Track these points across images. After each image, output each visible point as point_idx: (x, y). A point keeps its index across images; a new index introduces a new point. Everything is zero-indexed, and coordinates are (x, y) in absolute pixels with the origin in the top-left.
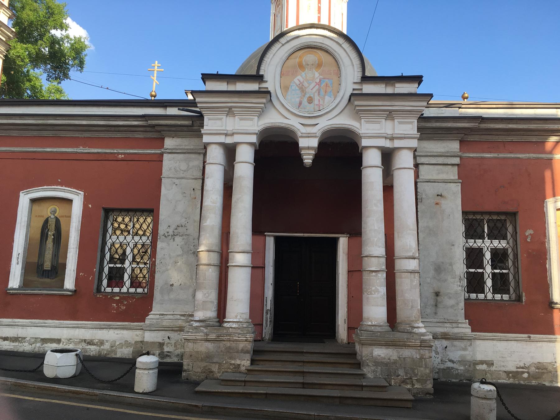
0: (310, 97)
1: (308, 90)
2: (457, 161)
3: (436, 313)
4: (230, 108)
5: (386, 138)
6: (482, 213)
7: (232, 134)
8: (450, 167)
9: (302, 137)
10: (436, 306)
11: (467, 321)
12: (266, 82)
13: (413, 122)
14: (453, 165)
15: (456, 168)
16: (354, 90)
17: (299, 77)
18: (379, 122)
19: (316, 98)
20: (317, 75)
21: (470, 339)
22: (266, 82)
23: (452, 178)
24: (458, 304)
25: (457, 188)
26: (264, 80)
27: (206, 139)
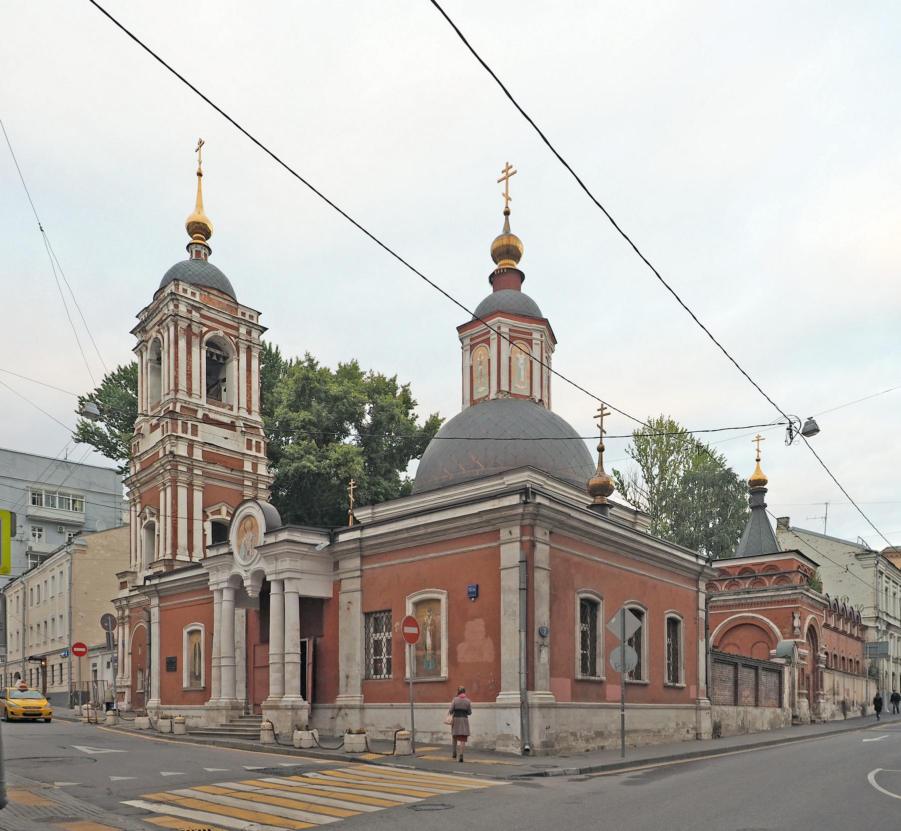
0: (248, 551)
1: (247, 546)
2: (358, 573)
3: (347, 691)
4: (216, 566)
5: (276, 573)
6: (380, 612)
7: (218, 584)
8: (356, 578)
9: (245, 579)
10: (347, 685)
11: (363, 695)
12: (231, 545)
13: (286, 560)
14: (358, 577)
15: (360, 578)
16: (265, 541)
17: (244, 538)
18: (273, 563)
19: (251, 551)
20: (251, 534)
21: (362, 708)
22: (231, 545)
23: (357, 587)
24: (357, 683)
25: (358, 595)
26: (230, 544)
27: (211, 588)
